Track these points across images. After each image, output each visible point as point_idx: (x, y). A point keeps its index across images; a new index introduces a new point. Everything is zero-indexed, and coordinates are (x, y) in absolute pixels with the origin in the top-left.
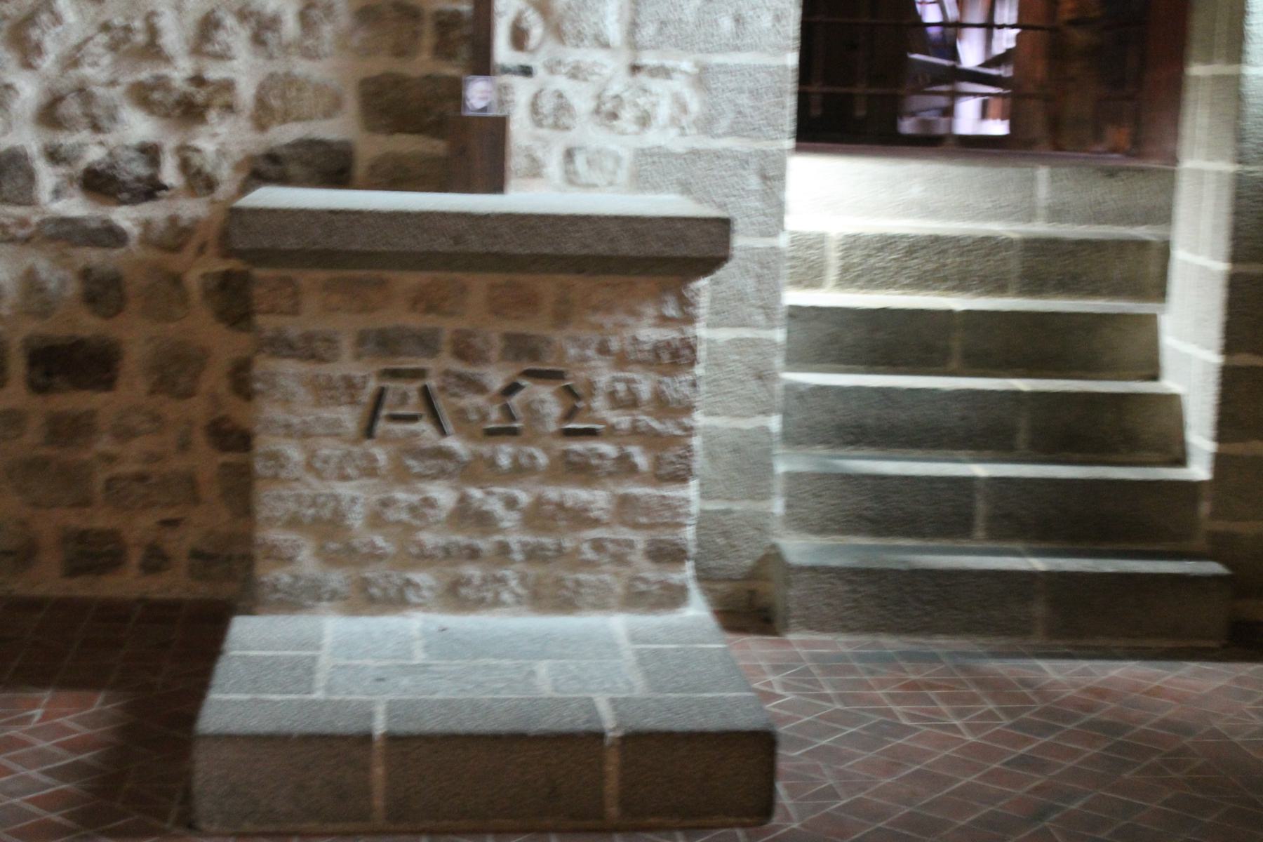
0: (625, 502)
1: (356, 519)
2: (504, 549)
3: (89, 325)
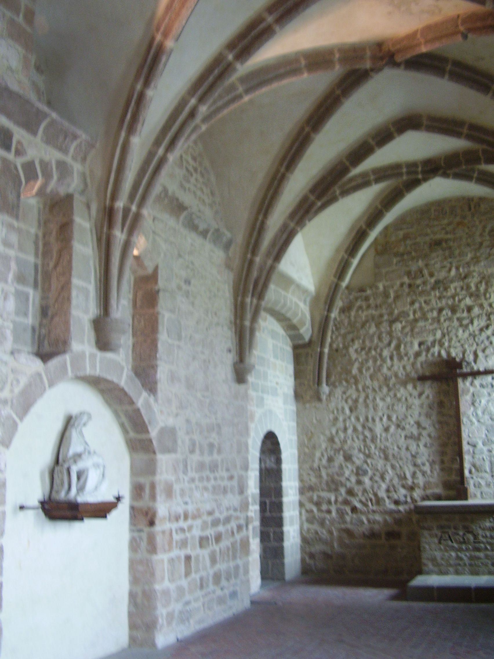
1: (439, 558)
2: (465, 565)
3: (396, 528)
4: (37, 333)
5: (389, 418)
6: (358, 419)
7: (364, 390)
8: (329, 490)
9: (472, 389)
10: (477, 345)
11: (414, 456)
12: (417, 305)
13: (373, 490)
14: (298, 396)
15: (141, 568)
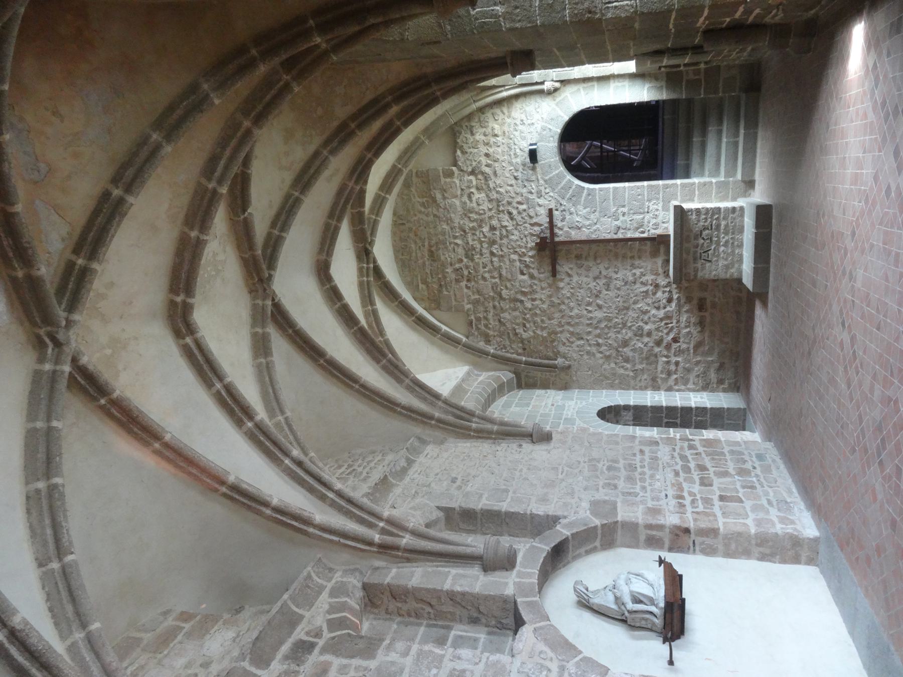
0: (724, 218)
1: (726, 263)
2: (732, 238)
3: (695, 302)
4: (495, 630)
5: (589, 304)
6: (590, 332)
8: (657, 362)
9: (566, 229)
11: (626, 283)
12: (487, 275)
13: (658, 322)
14: (565, 387)
15: (733, 546)
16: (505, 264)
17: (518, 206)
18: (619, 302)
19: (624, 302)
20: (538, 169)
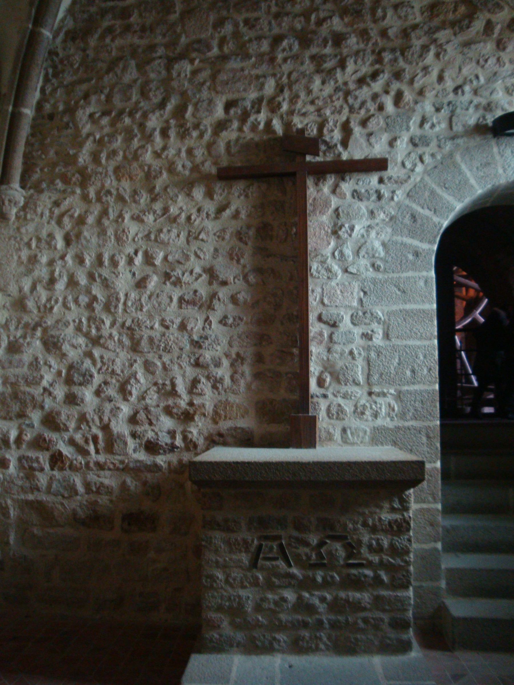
0: (377, 599)
1: (249, 608)
2: (320, 622)
5: (149, 259)
6: (80, 260)
7: (99, 199)
9: (334, 202)
10: (351, 109)
11: (197, 344)
12: (228, 28)
13: (101, 419)
16: (254, 66)
17: (393, 93)
18: (152, 328)
19: (151, 340)
20: (478, 140)
